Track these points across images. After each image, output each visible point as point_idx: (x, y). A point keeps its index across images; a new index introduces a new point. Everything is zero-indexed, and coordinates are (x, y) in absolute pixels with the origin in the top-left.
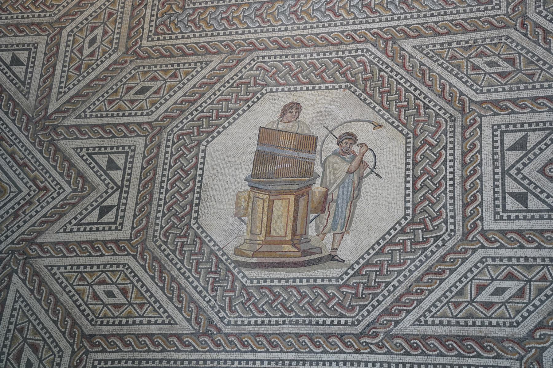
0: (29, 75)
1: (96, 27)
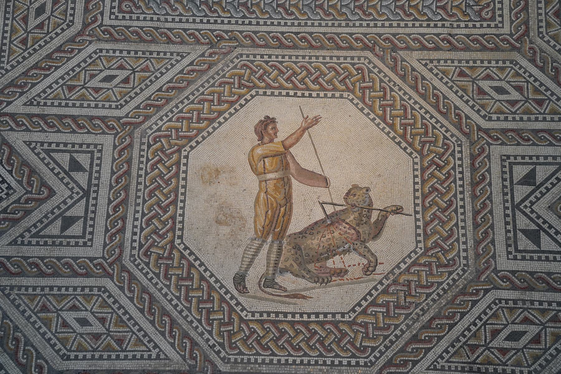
0: (550, 160)
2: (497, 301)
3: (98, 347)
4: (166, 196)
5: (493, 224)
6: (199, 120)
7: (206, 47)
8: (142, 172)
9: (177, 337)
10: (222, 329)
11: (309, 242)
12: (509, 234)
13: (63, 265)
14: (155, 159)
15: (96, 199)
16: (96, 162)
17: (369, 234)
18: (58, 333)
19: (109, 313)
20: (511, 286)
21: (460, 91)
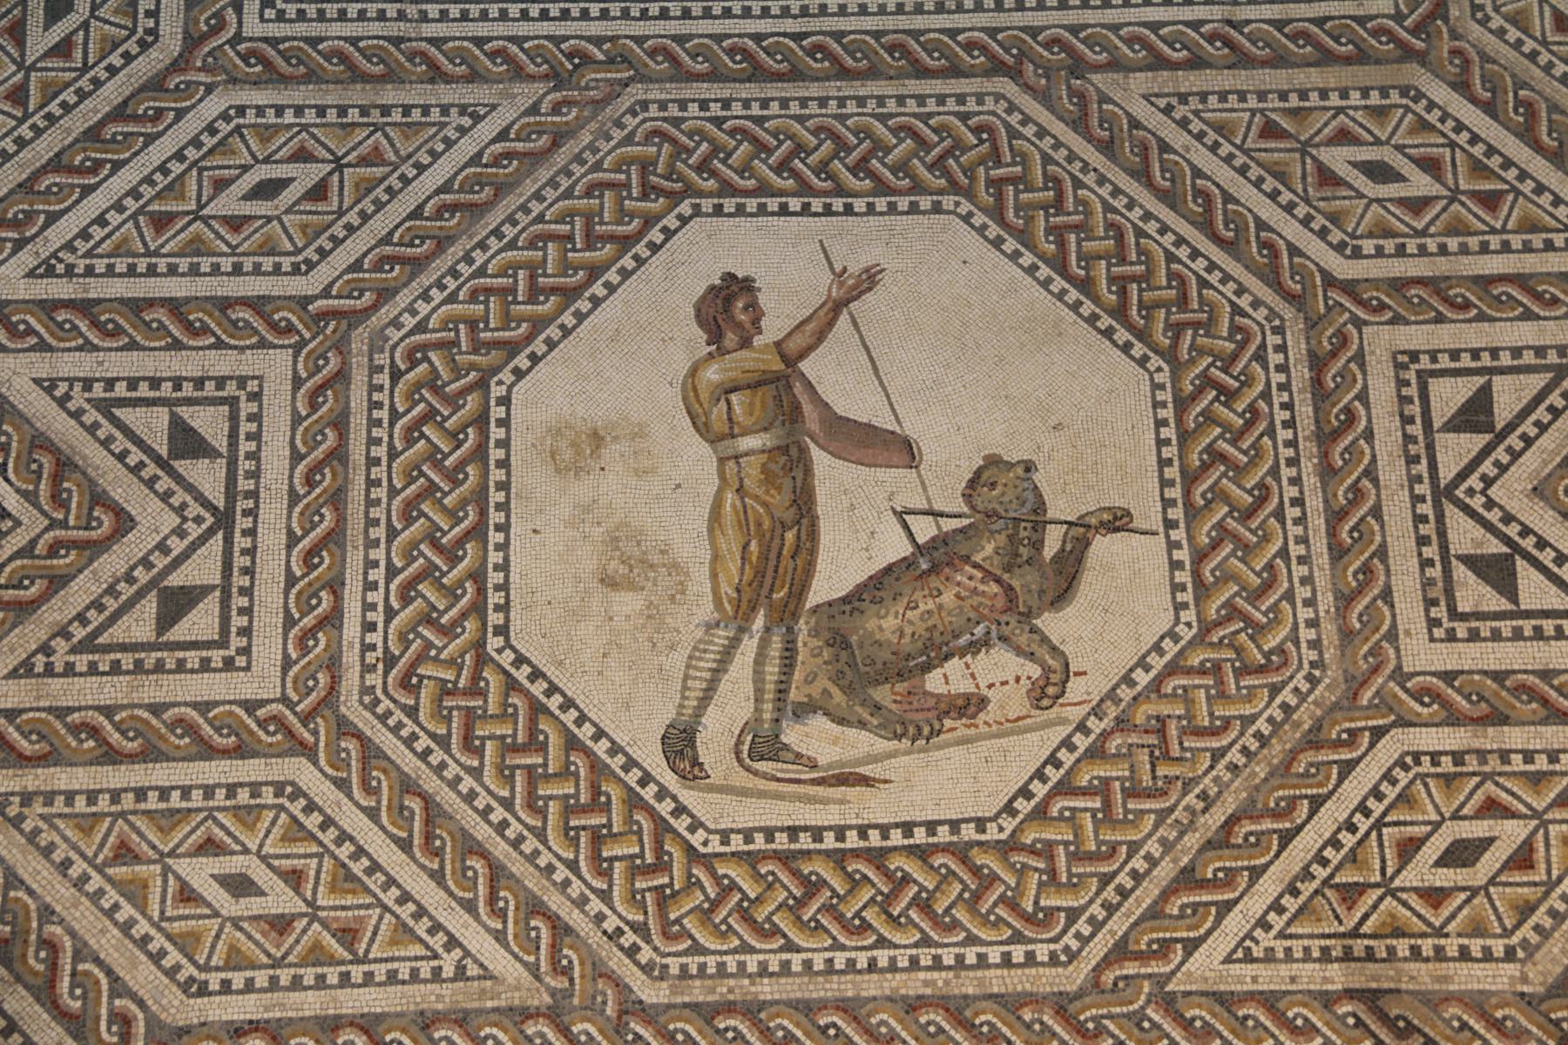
0: (1528, 358)
1: (1322, 169)
2: (1409, 760)
3: (287, 954)
4: (454, 516)
5: (1383, 546)
6: (534, 293)
7: (540, 88)
8: (380, 452)
9: (511, 914)
10: (638, 885)
11: (871, 624)
12: (1429, 572)
13: (172, 727)
14: (415, 412)
15: (251, 533)
16: (246, 427)
17: (1042, 592)
18: (169, 919)
19: (311, 856)
20: (1444, 714)
21: (1269, 179)
